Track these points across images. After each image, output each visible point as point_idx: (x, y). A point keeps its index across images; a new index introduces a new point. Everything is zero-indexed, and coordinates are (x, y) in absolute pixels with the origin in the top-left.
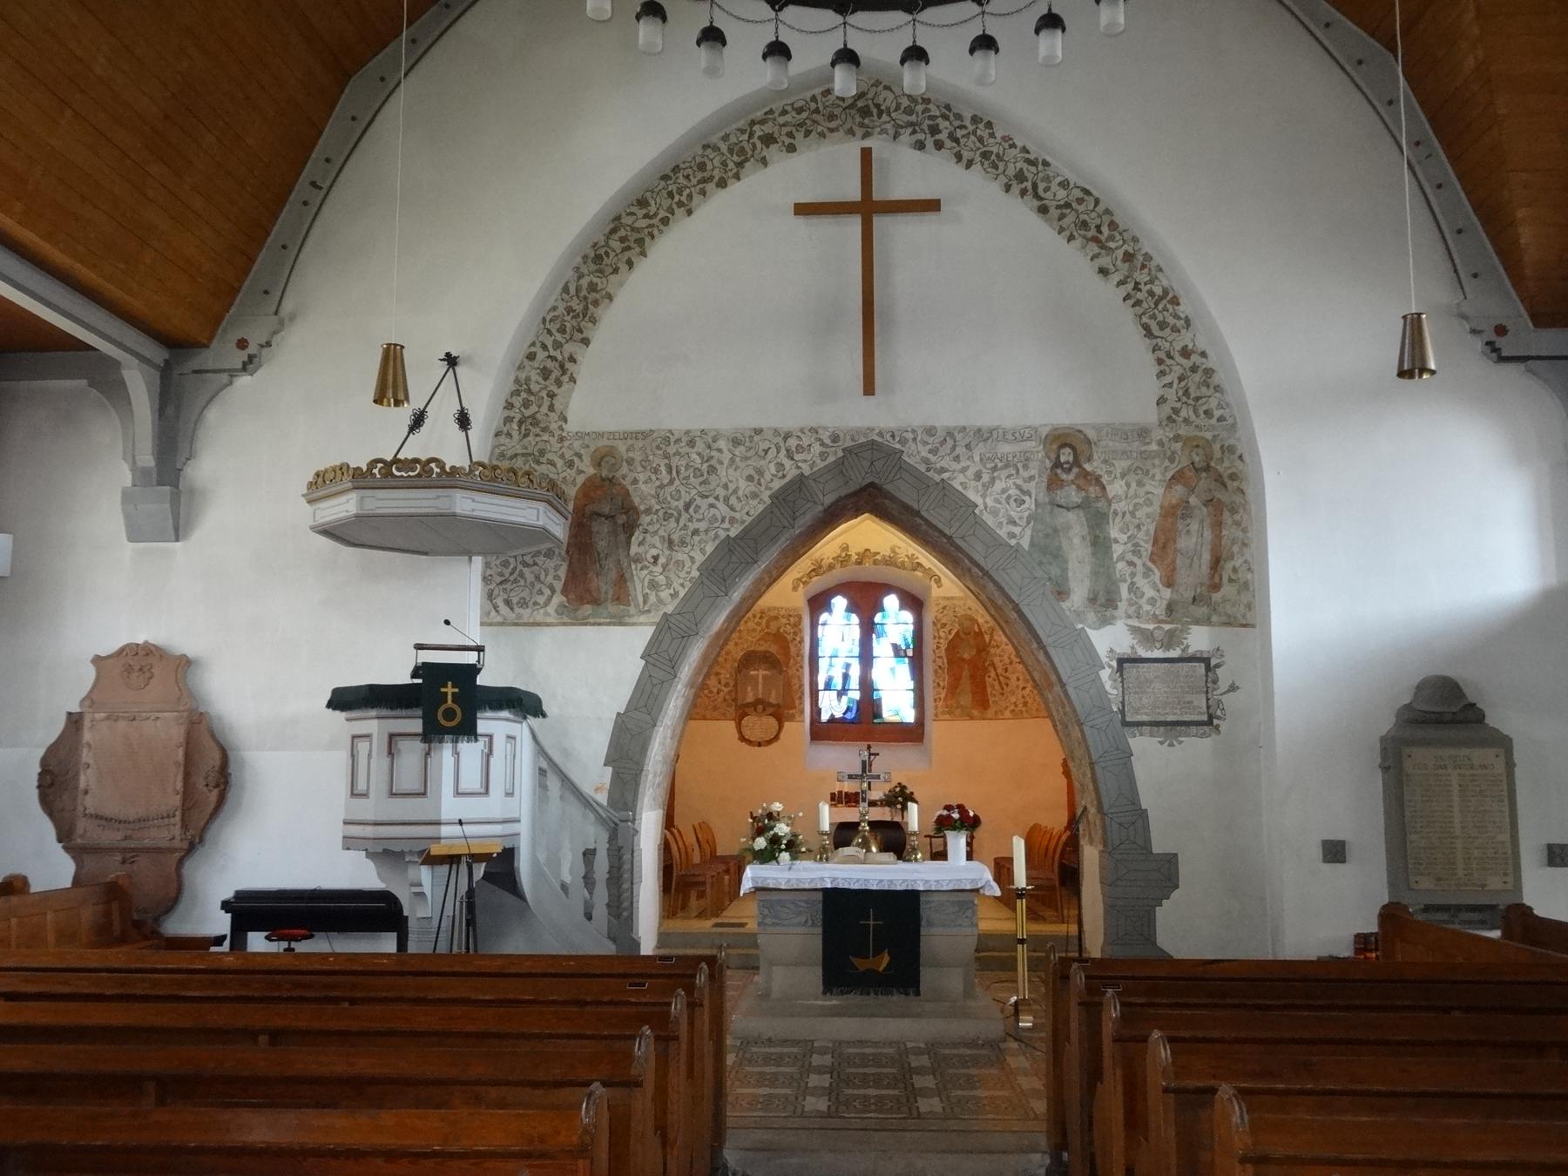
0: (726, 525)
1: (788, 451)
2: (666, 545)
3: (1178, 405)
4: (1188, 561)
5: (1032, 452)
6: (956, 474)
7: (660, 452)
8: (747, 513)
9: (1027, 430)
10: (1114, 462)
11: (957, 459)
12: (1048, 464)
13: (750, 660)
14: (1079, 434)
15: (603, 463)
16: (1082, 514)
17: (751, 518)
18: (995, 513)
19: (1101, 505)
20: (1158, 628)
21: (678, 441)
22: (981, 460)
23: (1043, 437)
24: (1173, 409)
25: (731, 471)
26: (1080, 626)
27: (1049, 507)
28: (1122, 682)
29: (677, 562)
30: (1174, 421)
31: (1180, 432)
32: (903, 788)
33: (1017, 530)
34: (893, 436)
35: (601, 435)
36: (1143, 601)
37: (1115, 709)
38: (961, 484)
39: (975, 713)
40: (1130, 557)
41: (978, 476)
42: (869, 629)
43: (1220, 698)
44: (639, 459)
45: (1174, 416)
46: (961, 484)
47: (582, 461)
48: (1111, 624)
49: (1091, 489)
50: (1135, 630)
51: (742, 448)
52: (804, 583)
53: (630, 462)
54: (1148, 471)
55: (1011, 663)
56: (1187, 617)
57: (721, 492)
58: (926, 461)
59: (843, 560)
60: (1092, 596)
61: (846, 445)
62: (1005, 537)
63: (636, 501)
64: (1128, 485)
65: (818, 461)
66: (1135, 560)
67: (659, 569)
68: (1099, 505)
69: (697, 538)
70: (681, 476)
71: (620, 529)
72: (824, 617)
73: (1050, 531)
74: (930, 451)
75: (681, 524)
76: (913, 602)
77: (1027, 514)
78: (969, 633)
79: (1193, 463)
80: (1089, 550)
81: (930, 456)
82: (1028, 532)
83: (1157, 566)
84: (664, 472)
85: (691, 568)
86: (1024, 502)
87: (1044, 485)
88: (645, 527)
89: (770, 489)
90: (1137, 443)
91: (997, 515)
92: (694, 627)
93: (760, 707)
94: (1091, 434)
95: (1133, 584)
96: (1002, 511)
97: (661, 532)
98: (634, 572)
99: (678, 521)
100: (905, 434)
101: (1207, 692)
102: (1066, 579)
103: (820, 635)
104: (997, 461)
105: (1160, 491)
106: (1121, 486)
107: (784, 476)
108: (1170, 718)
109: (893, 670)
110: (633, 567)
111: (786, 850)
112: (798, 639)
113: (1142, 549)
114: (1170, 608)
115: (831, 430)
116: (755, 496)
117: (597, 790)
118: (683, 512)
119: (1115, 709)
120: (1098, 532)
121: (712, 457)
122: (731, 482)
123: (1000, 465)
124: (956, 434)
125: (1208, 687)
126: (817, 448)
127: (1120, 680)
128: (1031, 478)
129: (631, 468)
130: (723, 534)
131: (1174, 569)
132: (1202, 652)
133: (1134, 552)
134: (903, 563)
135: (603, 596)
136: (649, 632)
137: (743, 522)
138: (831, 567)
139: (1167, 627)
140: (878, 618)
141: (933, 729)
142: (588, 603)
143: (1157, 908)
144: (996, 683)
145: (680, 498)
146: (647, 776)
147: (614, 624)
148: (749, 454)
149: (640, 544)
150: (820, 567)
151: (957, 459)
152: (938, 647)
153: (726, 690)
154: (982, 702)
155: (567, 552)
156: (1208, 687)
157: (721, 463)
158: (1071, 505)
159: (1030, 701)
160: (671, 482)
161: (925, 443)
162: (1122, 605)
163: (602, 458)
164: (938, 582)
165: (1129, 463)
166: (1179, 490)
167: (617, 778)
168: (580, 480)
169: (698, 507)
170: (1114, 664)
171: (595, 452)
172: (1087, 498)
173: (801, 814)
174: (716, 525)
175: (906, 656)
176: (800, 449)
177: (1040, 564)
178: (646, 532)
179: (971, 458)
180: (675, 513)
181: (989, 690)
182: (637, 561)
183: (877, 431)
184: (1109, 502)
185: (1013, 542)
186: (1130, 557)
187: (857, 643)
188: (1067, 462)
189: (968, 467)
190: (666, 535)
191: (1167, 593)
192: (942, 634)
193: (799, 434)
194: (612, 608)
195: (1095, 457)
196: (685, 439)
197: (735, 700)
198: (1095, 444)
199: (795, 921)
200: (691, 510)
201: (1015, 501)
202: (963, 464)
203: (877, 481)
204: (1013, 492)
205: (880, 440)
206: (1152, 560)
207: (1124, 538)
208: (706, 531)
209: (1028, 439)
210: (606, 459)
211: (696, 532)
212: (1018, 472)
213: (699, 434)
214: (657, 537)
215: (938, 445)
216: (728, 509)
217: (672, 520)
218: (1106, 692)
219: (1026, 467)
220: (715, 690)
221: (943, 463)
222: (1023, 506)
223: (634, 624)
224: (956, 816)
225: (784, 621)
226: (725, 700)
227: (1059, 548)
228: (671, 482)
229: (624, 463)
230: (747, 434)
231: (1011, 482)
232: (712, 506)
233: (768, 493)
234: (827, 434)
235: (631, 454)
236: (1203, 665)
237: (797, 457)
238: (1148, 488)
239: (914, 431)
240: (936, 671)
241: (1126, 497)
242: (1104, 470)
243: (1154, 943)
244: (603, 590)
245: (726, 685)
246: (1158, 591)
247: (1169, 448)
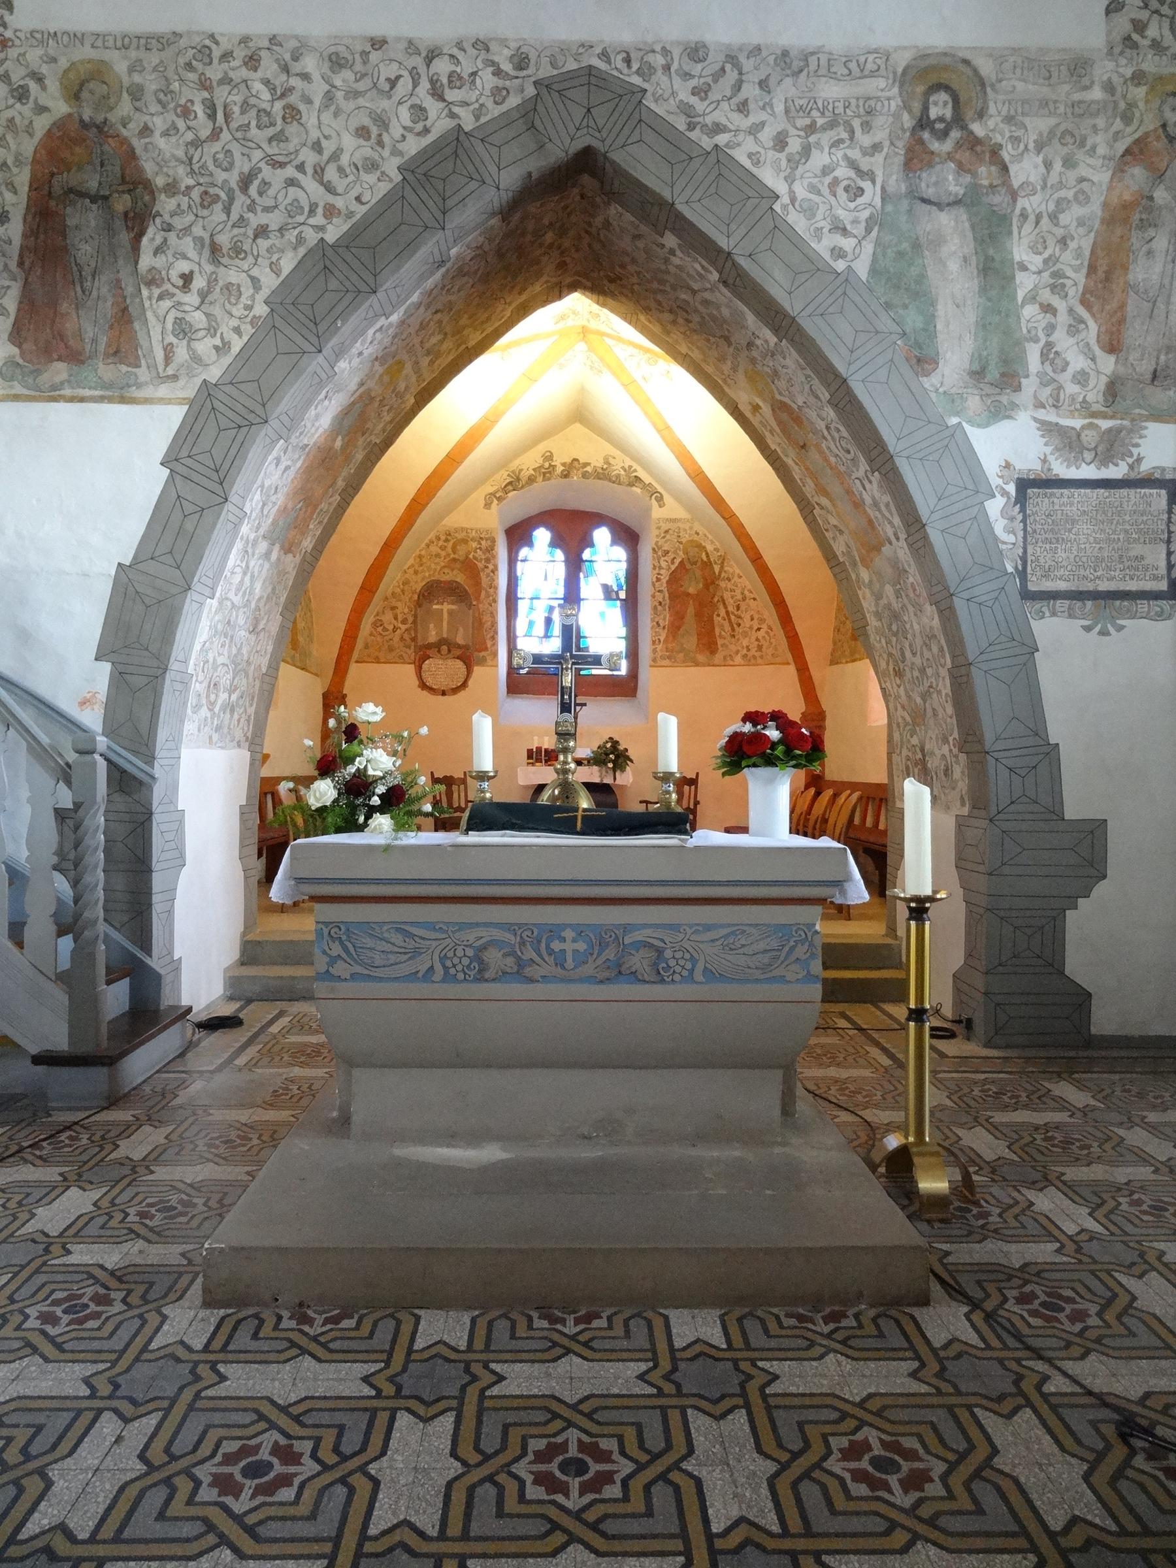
0: (318, 219)
1: (433, 82)
2: (206, 252)
3: (1144, 15)
4: (1147, 306)
5: (878, 99)
6: (740, 138)
7: (192, 76)
8: (358, 199)
9: (871, 57)
10: (1027, 120)
11: (743, 108)
12: (908, 121)
13: (432, 591)
14: (962, 67)
15: (85, 95)
16: (964, 217)
17: (363, 209)
18: (809, 212)
19: (999, 199)
20: (1091, 426)
21: (226, 56)
22: (787, 111)
23: (900, 70)
24: (1133, 21)
25: (327, 117)
26: (954, 421)
27: (905, 204)
28: (1024, 521)
29: (228, 287)
30: (1135, 46)
31: (1145, 66)
32: (615, 744)
33: (848, 244)
34: (628, 61)
35: (77, 38)
36: (1065, 378)
37: (1010, 569)
38: (750, 155)
39: (701, 658)
40: (1046, 296)
41: (780, 142)
42: (575, 566)
44: (154, 87)
45: (1135, 37)
46: (750, 155)
47: (44, 88)
48: (1009, 417)
49: (982, 170)
50: (1048, 429)
51: (347, 74)
52: (499, 499)
53: (136, 93)
54: (1082, 144)
55: (744, 599)
56: (1140, 407)
57: (309, 157)
58: (687, 110)
59: (546, 472)
60: (976, 367)
61: (541, 74)
62: (826, 256)
63: (149, 168)
64: (1048, 165)
65: (490, 104)
66: (1056, 302)
67: (192, 299)
68: (996, 199)
69: (263, 244)
70: (234, 125)
71: (119, 223)
72: (524, 552)
73: (905, 246)
74: (695, 92)
75: (234, 216)
76: (627, 536)
77: (866, 214)
78: (695, 563)
79: (1164, 126)
80: (975, 284)
81: (693, 100)
82: (868, 248)
83: (1093, 315)
84: (200, 114)
85: (253, 298)
86: (861, 191)
87: (899, 160)
88: (167, 217)
89: (401, 154)
90: (1066, 87)
91: (814, 216)
92: (259, 410)
93: (444, 648)
94: (986, 68)
95: (1049, 345)
96: (822, 209)
97: (197, 231)
98: (147, 304)
99: (227, 210)
100: (650, 58)
101: (1169, 542)
102: (930, 330)
103: (519, 573)
104: (815, 113)
105: (1103, 177)
106: (1036, 167)
107: (426, 131)
108: (1104, 586)
109: (602, 615)
110: (145, 292)
111: (382, 809)
112: (491, 567)
113: (1068, 283)
114: (1113, 390)
115: (514, 45)
116: (372, 166)
117: (83, 703)
118: (238, 192)
119: (1010, 569)
120: (991, 252)
121: (291, 90)
122: (326, 137)
123: (820, 122)
124: (742, 59)
126: (487, 80)
127: (1020, 517)
128: (876, 147)
129: (138, 104)
130: (312, 238)
131: (1122, 321)
132: (1163, 469)
133: (1053, 288)
134: (618, 476)
135: (88, 348)
136: (175, 415)
137: (350, 214)
138: (531, 480)
139: (1105, 424)
140: (587, 554)
141: (647, 675)
142: (60, 359)
143: (1069, 913)
144: (726, 624)
145: (232, 164)
146: (186, 684)
147: (110, 400)
148: (362, 86)
149: (157, 251)
150: (518, 479)
151: (743, 108)
152: (658, 580)
153: (404, 627)
154: (709, 644)
155: (21, 264)
157: (309, 101)
158: (945, 199)
159: (765, 644)
160: (215, 135)
161: (687, 76)
162: (1029, 385)
163: (82, 85)
164: (660, 499)
165: (1052, 121)
166: (1137, 174)
167: (119, 679)
168: (42, 124)
169: (265, 184)
170: (1011, 488)
171: (66, 72)
172: (974, 188)
173: (424, 730)
174: (301, 219)
175: (618, 598)
176: (455, 80)
177: (888, 306)
178: (168, 228)
179: (767, 106)
180: (223, 195)
181: (717, 630)
182: (150, 283)
183: (598, 50)
184: (1014, 195)
185: (840, 266)
186: (1046, 296)
187: (562, 582)
188: (941, 119)
189: (763, 124)
190: (206, 236)
191: (1108, 364)
192: (664, 564)
193: (455, 51)
194: (106, 371)
195: (992, 110)
196: (240, 54)
197: (414, 639)
198: (992, 86)
199: (405, 969)
200: (253, 190)
201: (846, 189)
202: (755, 117)
203: (596, 144)
204: (843, 172)
205: (602, 66)
206: (1084, 302)
207: (1036, 261)
208: (281, 230)
209: (874, 74)
210: (91, 85)
211: (262, 232)
212: (852, 138)
213: (266, 44)
214: (189, 239)
215: (709, 80)
216: (322, 189)
217: (218, 207)
218: (996, 539)
219: (867, 127)
220: (391, 628)
221: (718, 116)
222: (860, 200)
223: (147, 401)
224: (774, 734)
225: (474, 545)
226: (402, 639)
227: (922, 278)
228: (215, 135)
229: (125, 95)
230: (359, 48)
231: (840, 154)
232: (291, 182)
233: (397, 161)
234: (507, 53)
235: (137, 78)
236: (1163, 492)
237: (451, 95)
238: (1082, 170)
239: (665, 52)
240: (655, 608)
241: (1044, 187)
242: (1008, 134)
243: (1063, 973)
244: (89, 333)
245: (404, 622)
246: (1093, 359)
247: (1124, 97)
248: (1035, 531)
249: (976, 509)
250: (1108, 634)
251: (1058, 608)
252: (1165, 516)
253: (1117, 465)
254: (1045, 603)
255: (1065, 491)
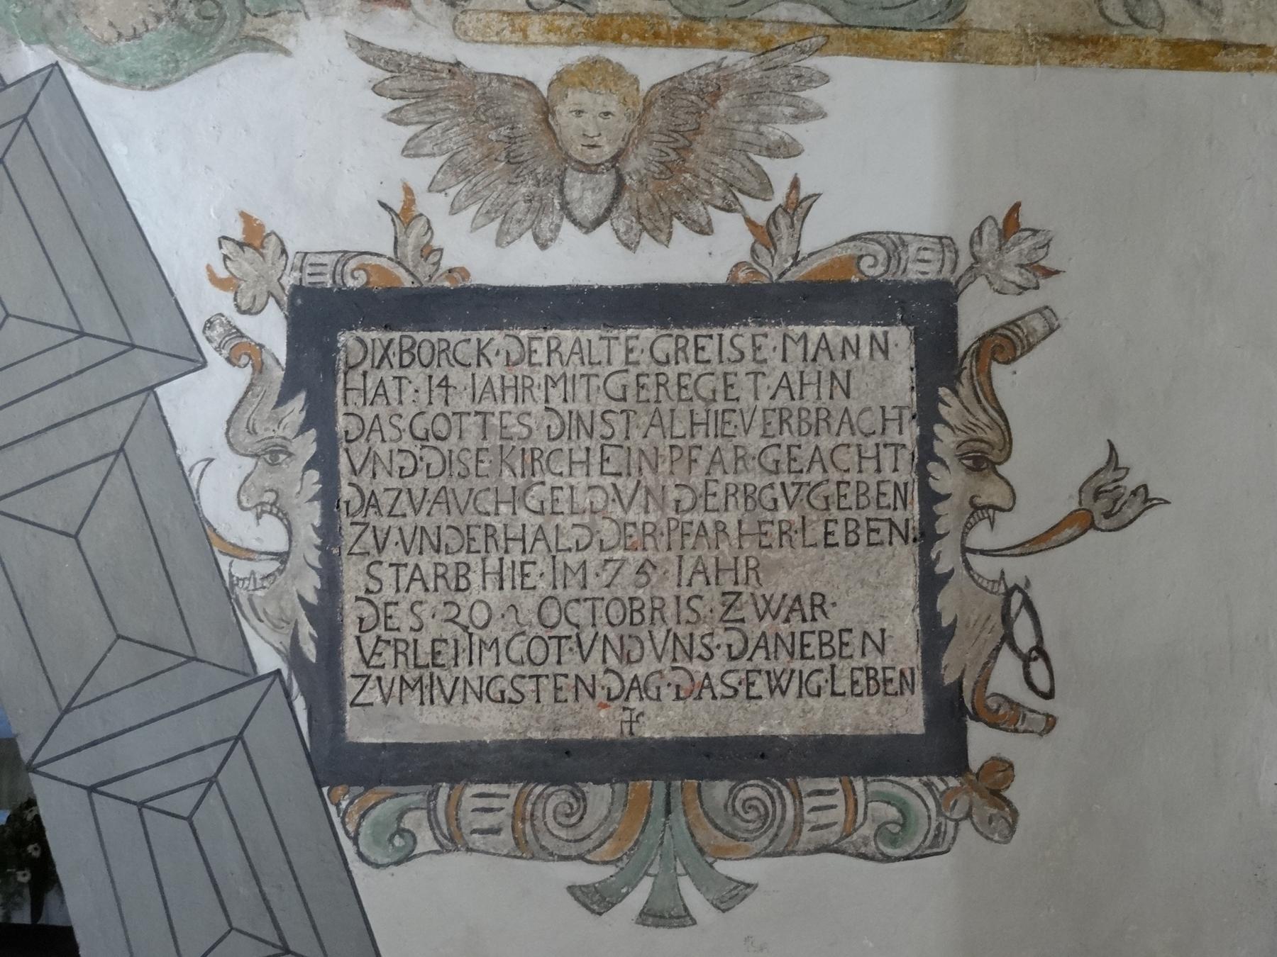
26: (31, 59)
28: (325, 462)
37: (268, 659)
43: (1016, 569)
101: (927, 536)
119: (268, 659)
125: (930, 498)
127: (307, 446)
132: (895, 244)
156: (930, 498)
218: (205, 532)
236: (900, 336)
248: (370, 502)
249: (120, 418)
250: (683, 918)
251: (470, 820)
252: (911, 433)
253: (705, 229)
254: (415, 796)
255: (497, 339)
